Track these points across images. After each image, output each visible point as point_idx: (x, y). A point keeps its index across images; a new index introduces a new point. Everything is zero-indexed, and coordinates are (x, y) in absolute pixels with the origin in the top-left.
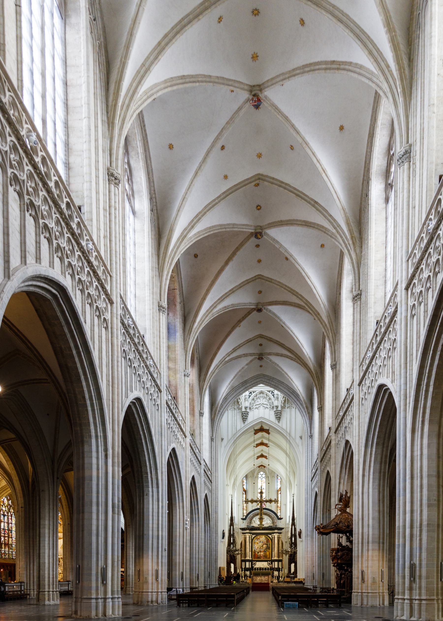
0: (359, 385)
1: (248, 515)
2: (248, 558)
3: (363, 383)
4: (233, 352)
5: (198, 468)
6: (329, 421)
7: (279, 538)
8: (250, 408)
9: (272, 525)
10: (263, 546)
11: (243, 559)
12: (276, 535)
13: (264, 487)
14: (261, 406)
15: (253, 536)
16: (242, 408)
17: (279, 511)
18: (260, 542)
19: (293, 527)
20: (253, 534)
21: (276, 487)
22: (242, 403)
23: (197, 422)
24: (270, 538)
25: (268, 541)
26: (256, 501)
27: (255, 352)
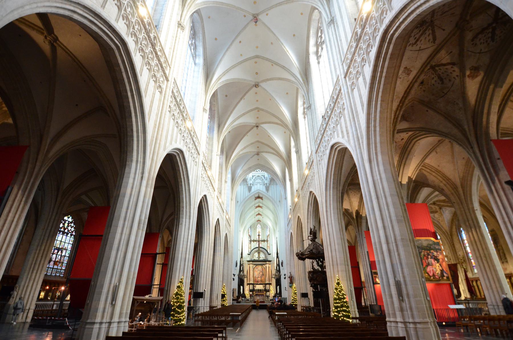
0: (316, 153)
2: (251, 282)
3: (319, 151)
5: (222, 214)
6: (296, 186)
11: (248, 282)
12: (267, 265)
13: (260, 232)
17: (269, 249)
20: (254, 264)
23: (223, 186)
25: (263, 270)
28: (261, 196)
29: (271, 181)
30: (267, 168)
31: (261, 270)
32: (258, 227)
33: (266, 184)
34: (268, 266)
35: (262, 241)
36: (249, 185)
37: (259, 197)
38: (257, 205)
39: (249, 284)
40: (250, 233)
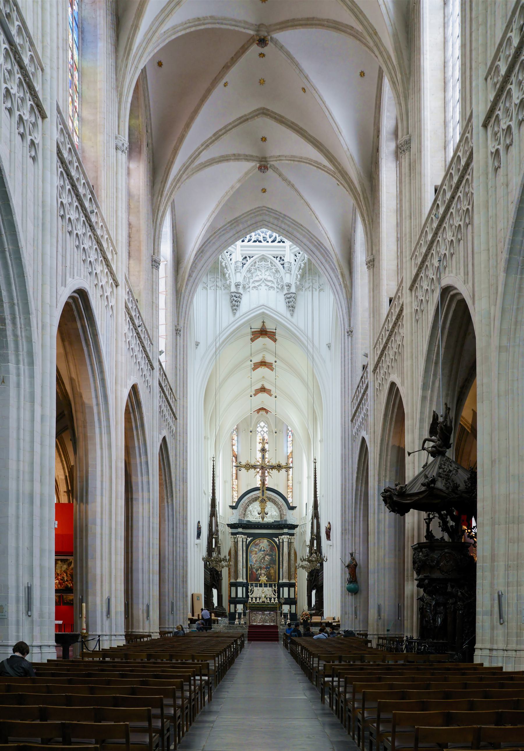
1: (240, 499)
2: (240, 580)
4: (213, 141)
7: (290, 544)
8: (244, 287)
9: (278, 519)
10: (264, 558)
11: (233, 581)
12: (285, 538)
14: (263, 285)
15: (249, 539)
16: (230, 286)
18: (260, 550)
19: (315, 521)
20: (249, 535)
21: (285, 449)
22: (231, 276)
24: (275, 543)
25: (272, 549)
26: (254, 467)
27: (254, 154)
28: (270, 327)
29: (303, 276)
30: (295, 223)
31: (268, 548)
32: (259, 429)
33: (289, 286)
34: (285, 540)
35: (272, 467)
36: (233, 289)
37: (263, 332)
38: (257, 359)
39: (235, 585)
40: (235, 448)
